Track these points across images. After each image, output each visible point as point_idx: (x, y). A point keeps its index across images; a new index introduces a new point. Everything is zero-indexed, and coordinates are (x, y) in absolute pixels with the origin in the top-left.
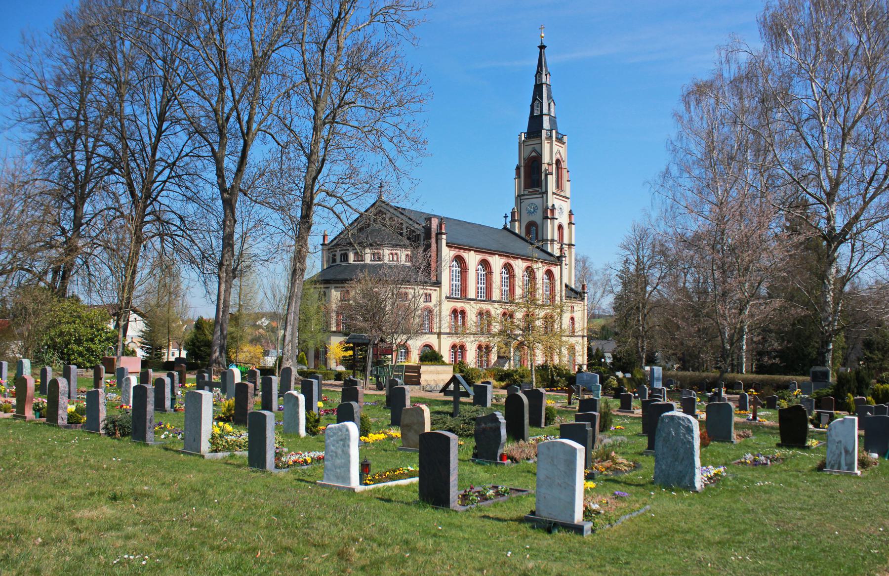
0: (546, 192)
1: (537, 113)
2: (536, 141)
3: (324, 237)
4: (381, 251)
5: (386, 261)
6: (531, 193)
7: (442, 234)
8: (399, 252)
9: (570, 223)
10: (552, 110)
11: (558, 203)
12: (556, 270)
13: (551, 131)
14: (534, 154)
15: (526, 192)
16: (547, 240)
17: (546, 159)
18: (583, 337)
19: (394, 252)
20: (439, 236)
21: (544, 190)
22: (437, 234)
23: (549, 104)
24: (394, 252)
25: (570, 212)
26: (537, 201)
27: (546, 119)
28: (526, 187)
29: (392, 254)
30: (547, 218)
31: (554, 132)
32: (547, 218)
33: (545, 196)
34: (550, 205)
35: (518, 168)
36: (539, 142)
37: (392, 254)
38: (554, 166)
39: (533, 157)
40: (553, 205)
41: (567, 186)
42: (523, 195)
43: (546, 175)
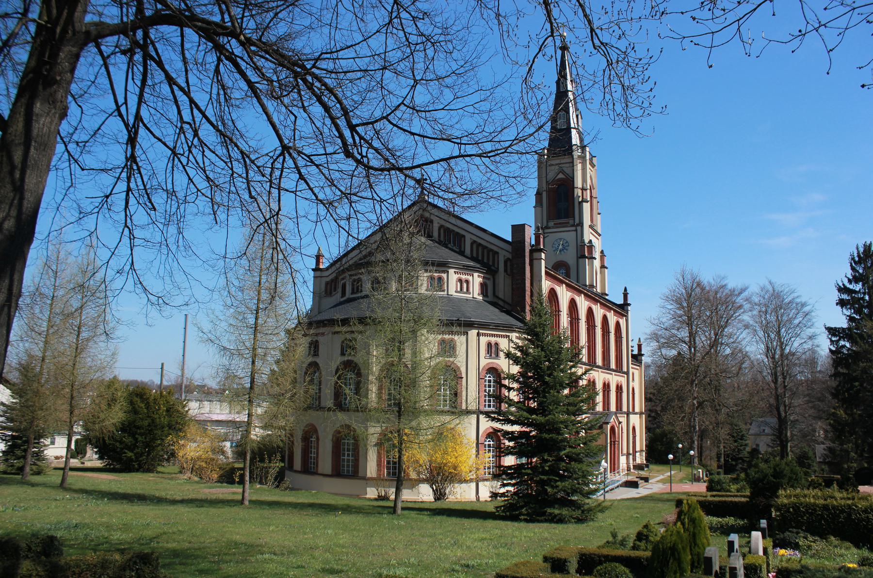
0: (581, 224)
1: (560, 124)
2: (566, 159)
3: (318, 257)
4: (444, 276)
5: (452, 291)
6: (557, 226)
7: (541, 250)
8: (470, 278)
9: (603, 267)
10: (580, 124)
11: (595, 242)
12: (622, 322)
13: (583, 148)
14: (561, 176)
15: (551, 224)
16: (586, 285)
17: (579, 183)
18: (641, 413)
19: (464, 277)
20: (536, 255)
21: (577, 221)
22: (531, 252)
23: (577, 116)
24: (464, 277)
25: (602, 252)
26: (570, 236)
27: (574, 132)
28: (549, 218)
29: (460, 280)
30: (584, 257)
31: (587, 149)
32: (584, 257)
33: (579, 228)
34: (586, 241)
35: (538, 194)
36: (569, 160)
37: (460, 280)
38: (588, 191)
39: (559, 180)
40: (590, 241)
41: (598, 219)
42: (547, 227)
43: (580, 203)
